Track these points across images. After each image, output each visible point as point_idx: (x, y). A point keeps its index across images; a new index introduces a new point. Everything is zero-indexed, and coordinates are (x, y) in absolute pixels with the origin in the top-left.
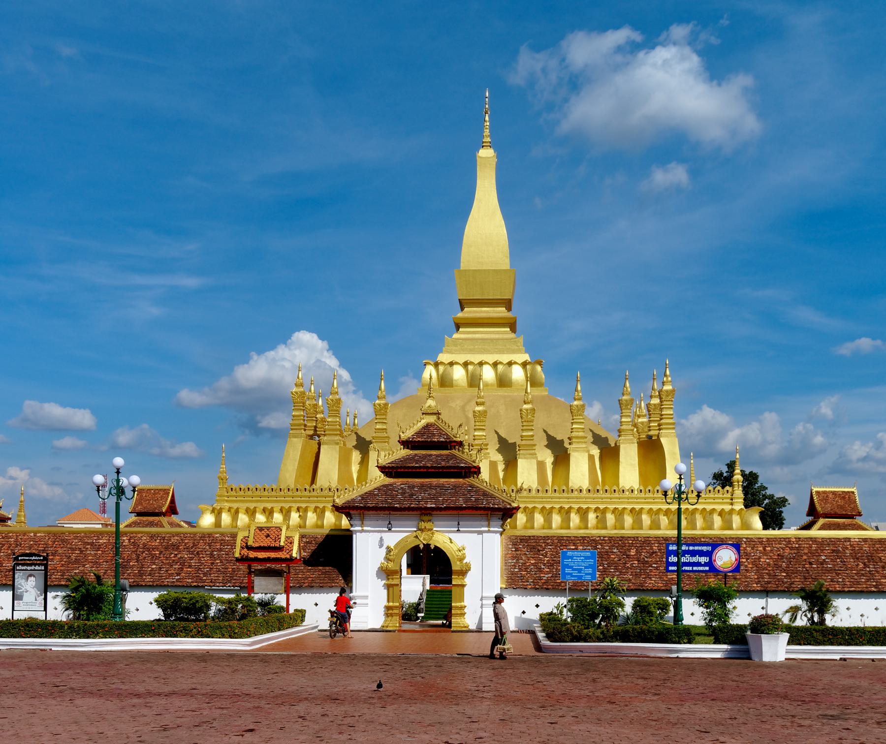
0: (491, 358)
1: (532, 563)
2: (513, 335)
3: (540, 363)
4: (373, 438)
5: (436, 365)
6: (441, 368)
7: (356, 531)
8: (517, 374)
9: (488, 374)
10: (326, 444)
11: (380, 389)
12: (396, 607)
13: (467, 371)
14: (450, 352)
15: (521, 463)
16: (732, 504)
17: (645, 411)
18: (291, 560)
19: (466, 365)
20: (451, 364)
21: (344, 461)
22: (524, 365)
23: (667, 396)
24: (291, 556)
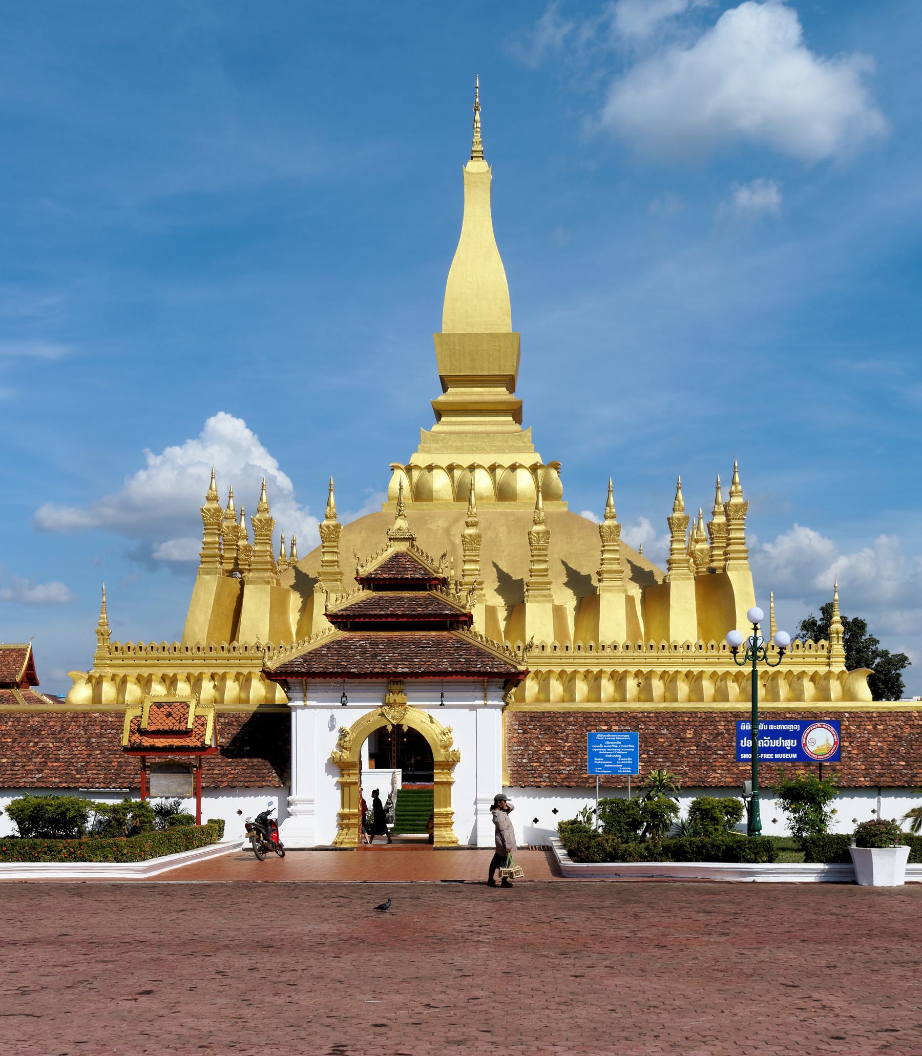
0: (487, 460)
1: (546, 752)
2: (517, 427)
3: (556, 466)
4: (319, 574)
5: (409, 469)
6: (416, 474)
7: (296, 708)
8: (524, 482)
9: (483, 483)
10: (252, 583)
11: (329, 504)
12: (354, 815)
13: (452, 478)
14: (428, 451)
15: (532, 609)
16: (829, 665)
17: (705, 534)
18: (204, 748)
19: (450, 469)
20: (430, 468)
21: (278, 607)
22: (534, 469)
23: (736, 512)
24: (203, 743)
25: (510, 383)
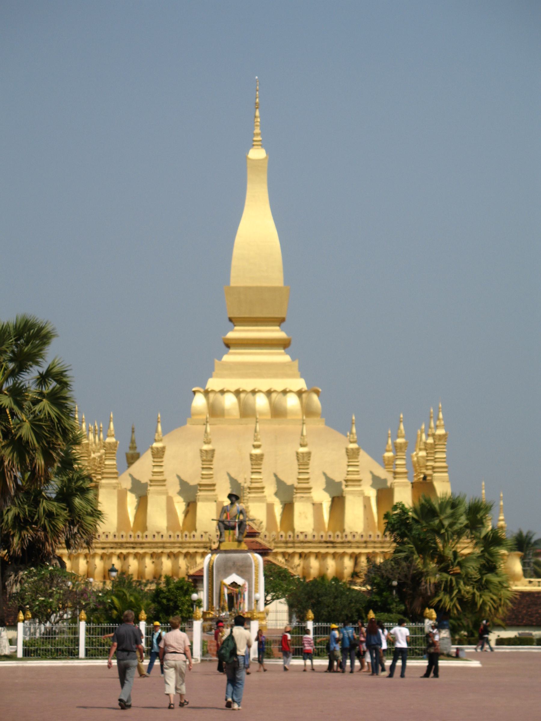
3: (317, 392)
4: (151, 481)
5: (207, 393)
6: (211, 396)
8: (292, 402)
10: (104, 486)
11: (156, 431)
22: (300, 393)
25: (280, 321)
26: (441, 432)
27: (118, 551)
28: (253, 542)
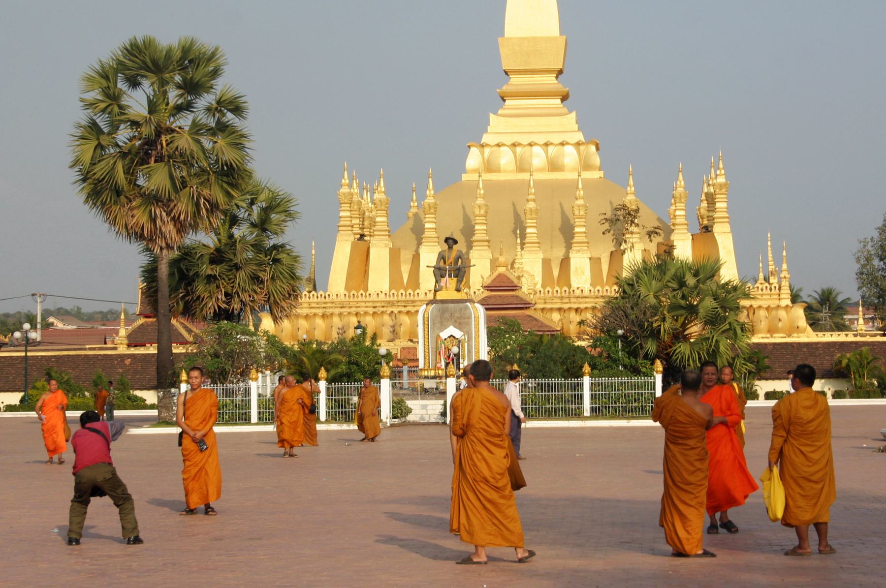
0: (541, 139)
2: (565, 110)
6: (487, 150)
8: (570, 156)
9: (538, 157)
13: (515, 153)
22: (578, 144)
26: (721, 180)
27: (389, 310)
28: (513, 296)
